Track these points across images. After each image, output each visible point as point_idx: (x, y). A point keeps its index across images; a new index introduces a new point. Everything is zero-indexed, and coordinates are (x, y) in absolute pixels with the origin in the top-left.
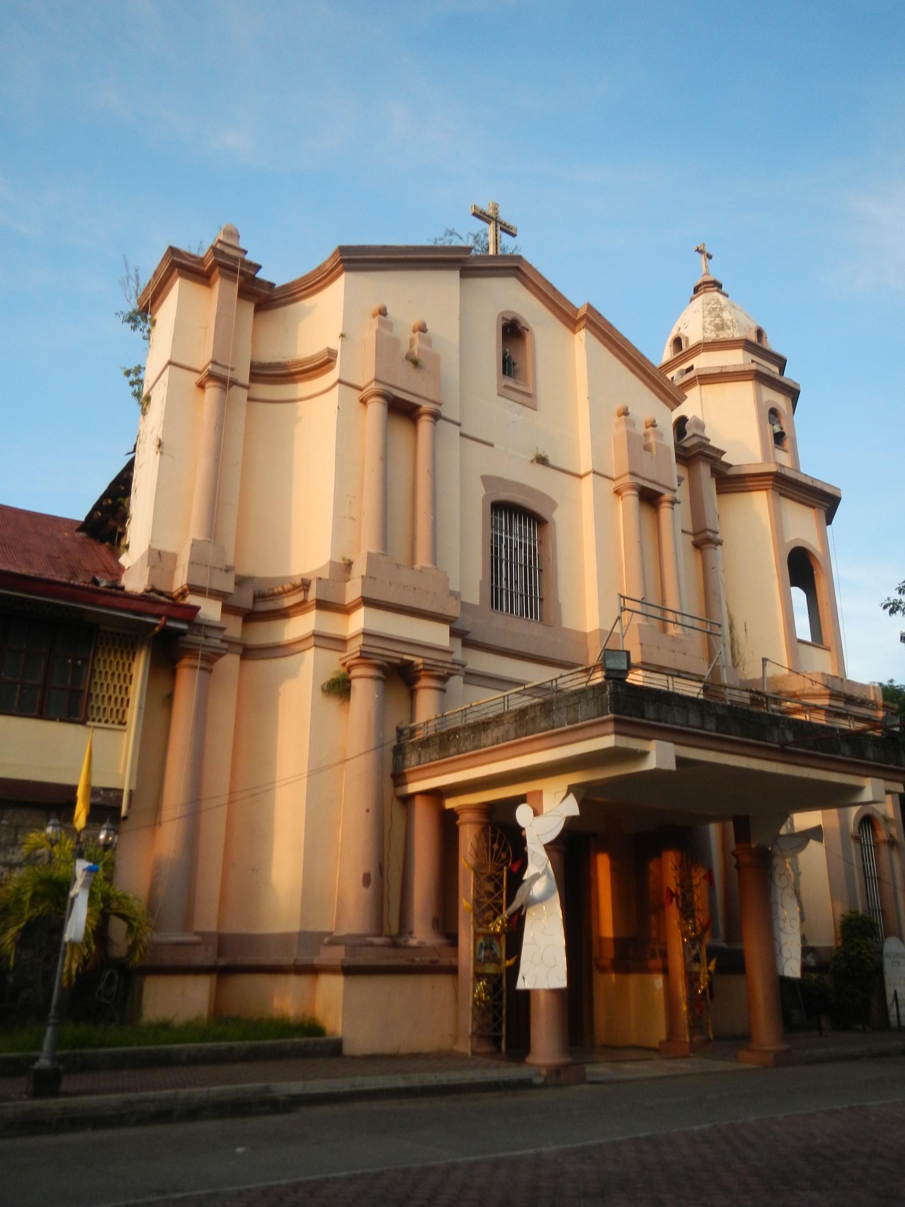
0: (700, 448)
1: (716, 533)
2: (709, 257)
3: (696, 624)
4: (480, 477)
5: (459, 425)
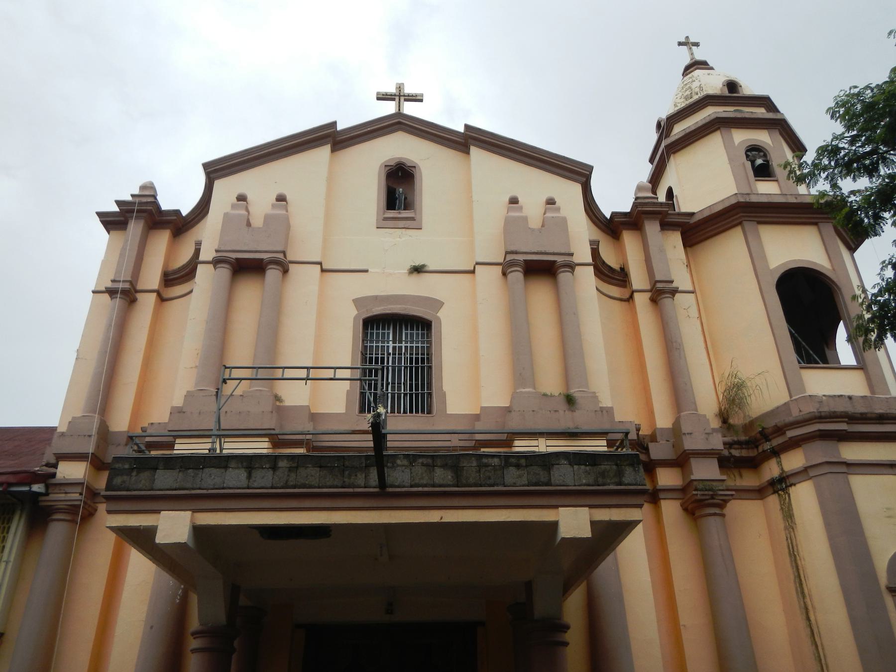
0: (637, 208)
1: (672, 282)
2: (697, 44)
3: (289, 373)
4: (352, 301)
5: (320, 264)
